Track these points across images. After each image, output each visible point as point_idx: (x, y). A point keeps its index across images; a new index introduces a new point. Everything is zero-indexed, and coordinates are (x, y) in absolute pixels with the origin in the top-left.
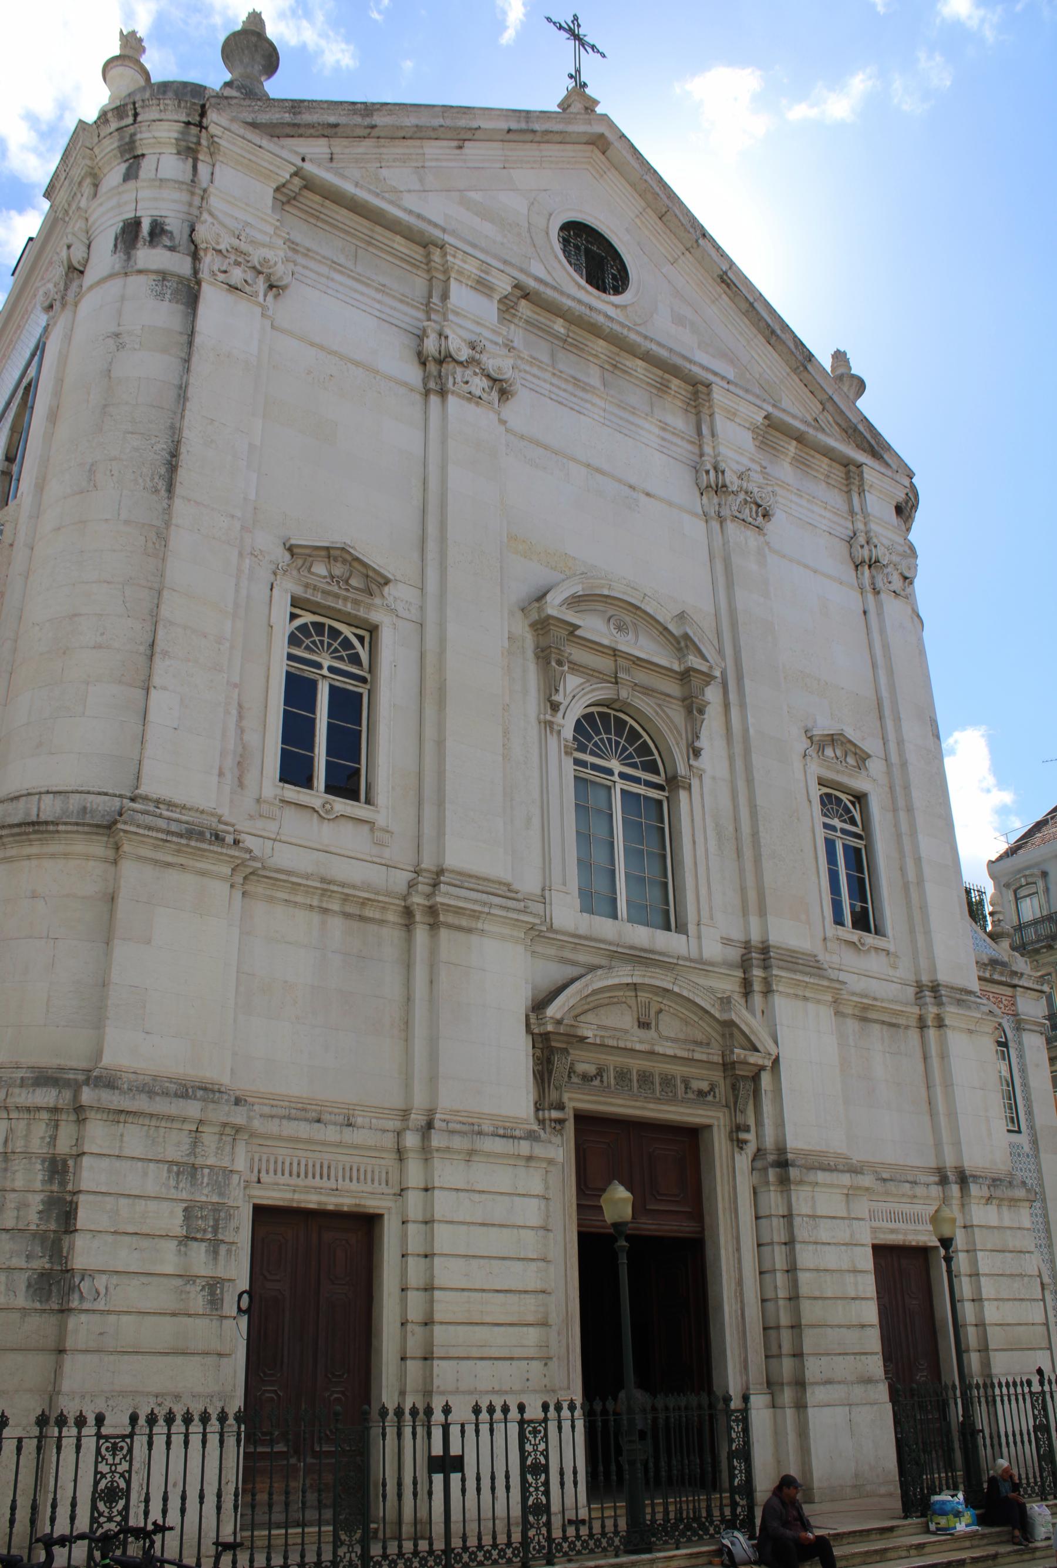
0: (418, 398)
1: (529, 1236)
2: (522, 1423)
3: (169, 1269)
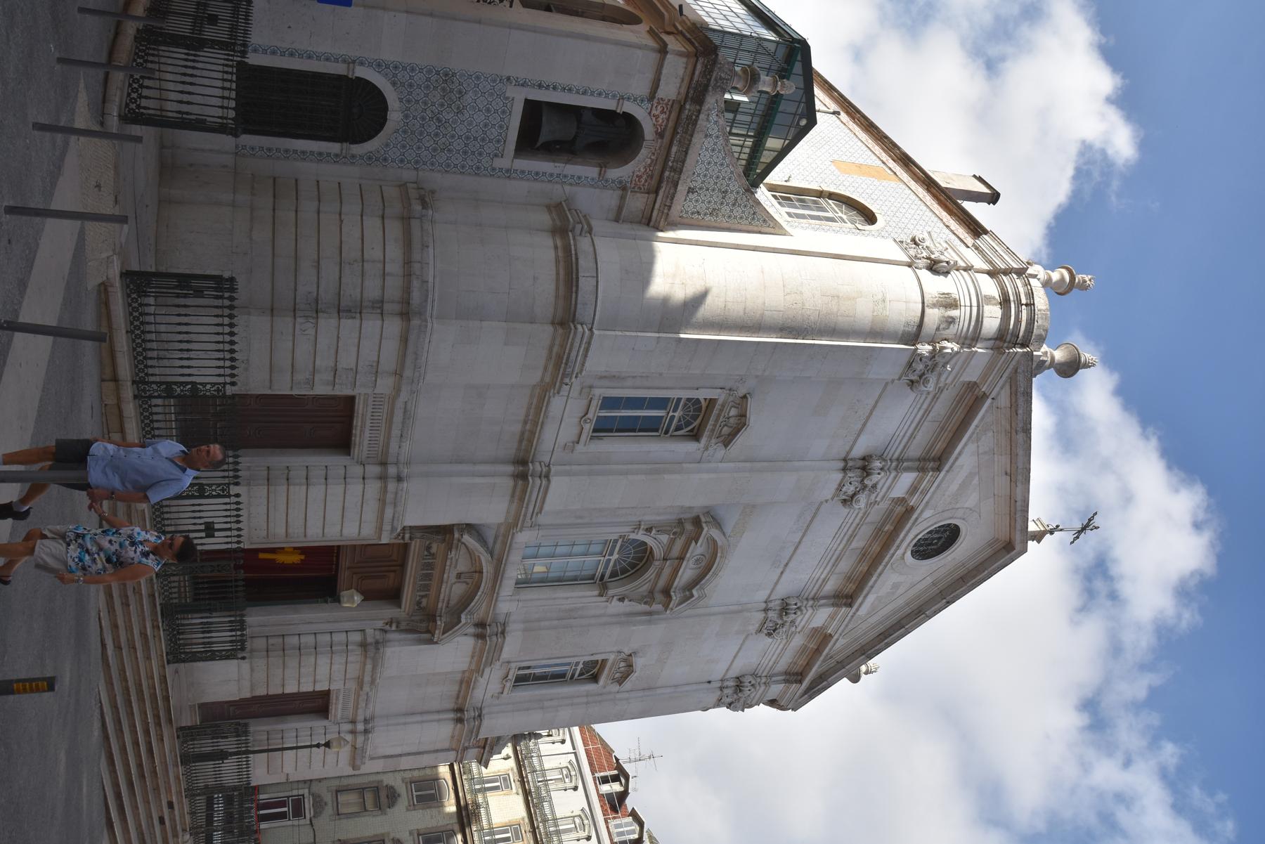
3: (318, 362)
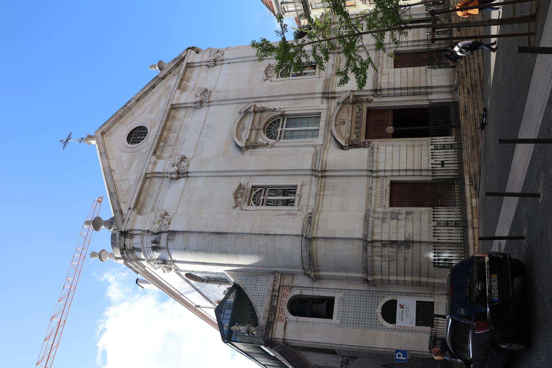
0: (189, 179)
1: (395, 149)
2: (435, 149)
3: (404, 222)
